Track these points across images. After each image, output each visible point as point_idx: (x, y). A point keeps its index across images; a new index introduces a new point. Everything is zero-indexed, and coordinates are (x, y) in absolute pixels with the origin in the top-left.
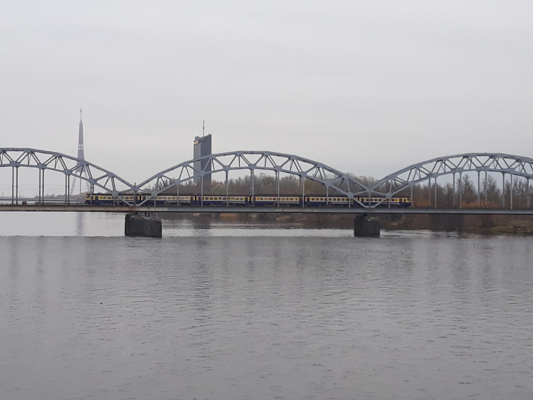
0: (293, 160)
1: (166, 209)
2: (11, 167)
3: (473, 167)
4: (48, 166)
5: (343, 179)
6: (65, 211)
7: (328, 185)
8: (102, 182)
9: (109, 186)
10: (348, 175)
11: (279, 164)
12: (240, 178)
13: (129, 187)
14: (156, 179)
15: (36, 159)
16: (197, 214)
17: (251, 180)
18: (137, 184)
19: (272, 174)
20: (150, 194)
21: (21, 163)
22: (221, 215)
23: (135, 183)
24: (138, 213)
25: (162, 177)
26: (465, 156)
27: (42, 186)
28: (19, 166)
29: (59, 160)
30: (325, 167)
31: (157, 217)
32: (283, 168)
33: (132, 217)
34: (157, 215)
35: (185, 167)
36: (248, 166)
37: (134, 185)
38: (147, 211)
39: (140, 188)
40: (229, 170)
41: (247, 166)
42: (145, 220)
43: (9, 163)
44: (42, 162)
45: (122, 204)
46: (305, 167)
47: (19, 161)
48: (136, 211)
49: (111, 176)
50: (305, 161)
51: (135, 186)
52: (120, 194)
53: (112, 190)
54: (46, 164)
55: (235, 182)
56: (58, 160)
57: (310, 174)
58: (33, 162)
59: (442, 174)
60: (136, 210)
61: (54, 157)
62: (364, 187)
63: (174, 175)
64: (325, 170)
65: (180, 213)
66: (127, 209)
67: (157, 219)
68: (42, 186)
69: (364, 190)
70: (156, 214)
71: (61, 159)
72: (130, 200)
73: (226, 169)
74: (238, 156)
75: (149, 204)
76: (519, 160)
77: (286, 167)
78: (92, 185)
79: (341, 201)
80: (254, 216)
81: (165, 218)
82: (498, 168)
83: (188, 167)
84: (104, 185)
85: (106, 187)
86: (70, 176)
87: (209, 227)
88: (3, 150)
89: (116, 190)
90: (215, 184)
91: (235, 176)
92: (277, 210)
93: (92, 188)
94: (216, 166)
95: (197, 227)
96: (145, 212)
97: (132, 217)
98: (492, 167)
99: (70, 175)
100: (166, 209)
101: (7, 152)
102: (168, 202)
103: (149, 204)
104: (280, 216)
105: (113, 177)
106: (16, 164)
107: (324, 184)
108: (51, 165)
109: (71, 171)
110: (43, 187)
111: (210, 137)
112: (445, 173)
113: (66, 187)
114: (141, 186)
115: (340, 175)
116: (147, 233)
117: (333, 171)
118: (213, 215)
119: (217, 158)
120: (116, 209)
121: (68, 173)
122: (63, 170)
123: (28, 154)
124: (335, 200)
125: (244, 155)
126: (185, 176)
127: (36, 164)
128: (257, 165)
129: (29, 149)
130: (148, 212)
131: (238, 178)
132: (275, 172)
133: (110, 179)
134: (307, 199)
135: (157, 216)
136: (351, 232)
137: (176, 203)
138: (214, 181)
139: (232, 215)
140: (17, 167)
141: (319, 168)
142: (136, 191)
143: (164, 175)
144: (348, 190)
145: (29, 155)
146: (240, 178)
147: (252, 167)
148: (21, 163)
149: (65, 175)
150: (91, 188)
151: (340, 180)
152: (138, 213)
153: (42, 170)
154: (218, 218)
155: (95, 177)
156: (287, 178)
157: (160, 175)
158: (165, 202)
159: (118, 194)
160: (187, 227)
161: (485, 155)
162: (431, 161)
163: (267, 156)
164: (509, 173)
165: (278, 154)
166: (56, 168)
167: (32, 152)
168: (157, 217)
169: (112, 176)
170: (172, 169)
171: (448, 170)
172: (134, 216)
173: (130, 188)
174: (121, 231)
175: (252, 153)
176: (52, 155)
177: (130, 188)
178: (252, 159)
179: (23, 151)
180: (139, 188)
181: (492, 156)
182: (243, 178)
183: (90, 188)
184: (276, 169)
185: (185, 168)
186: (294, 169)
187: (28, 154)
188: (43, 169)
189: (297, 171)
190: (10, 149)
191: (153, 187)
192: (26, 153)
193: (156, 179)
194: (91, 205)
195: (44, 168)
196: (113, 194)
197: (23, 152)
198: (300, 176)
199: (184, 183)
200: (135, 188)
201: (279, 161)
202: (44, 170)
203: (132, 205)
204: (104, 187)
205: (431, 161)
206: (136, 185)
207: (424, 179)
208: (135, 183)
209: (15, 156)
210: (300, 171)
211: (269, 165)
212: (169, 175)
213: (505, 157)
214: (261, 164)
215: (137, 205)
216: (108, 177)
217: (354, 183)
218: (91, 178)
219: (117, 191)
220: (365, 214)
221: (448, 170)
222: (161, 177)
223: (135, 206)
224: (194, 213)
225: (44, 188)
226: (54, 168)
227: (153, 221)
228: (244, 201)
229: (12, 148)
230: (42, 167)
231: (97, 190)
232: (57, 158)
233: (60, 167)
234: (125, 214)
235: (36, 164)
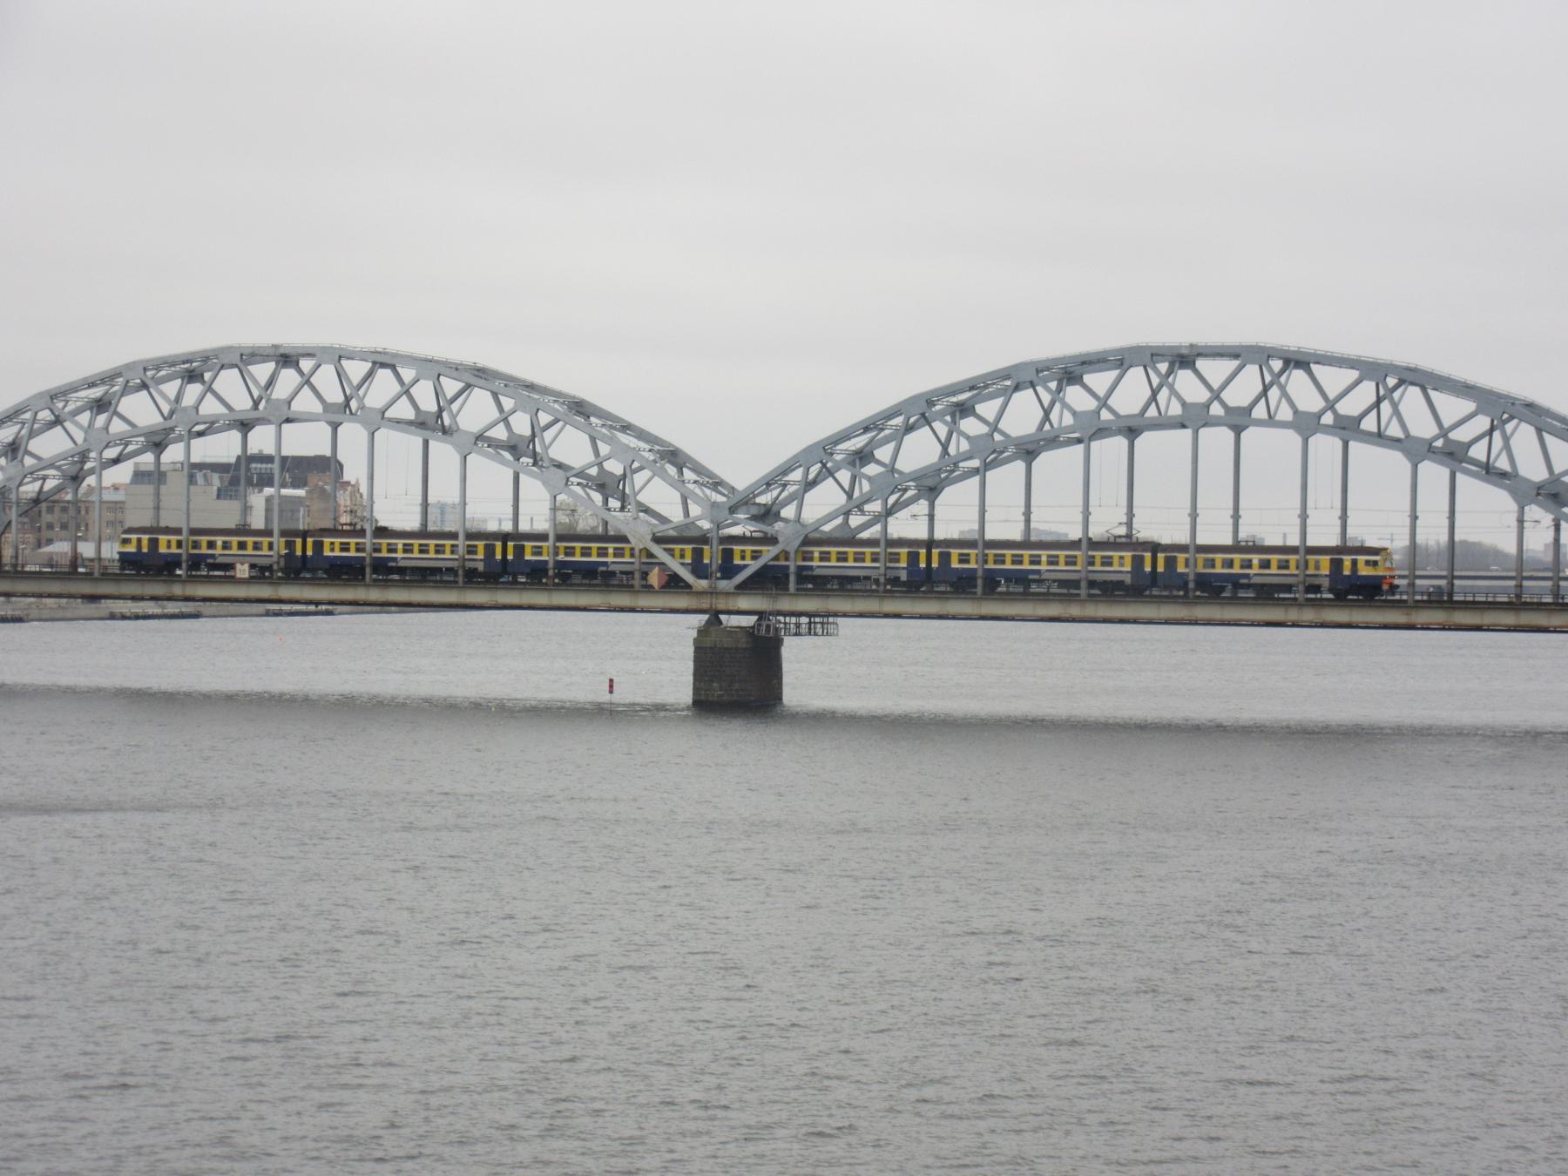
72: (434, 556)
79: (1274, 570)
102: (612, 568)
124: (1053, 561)
134: (515, 547)
137: (1288, 588)
194: (550, 582)
196: (634, 536)
228: (1127, 572)
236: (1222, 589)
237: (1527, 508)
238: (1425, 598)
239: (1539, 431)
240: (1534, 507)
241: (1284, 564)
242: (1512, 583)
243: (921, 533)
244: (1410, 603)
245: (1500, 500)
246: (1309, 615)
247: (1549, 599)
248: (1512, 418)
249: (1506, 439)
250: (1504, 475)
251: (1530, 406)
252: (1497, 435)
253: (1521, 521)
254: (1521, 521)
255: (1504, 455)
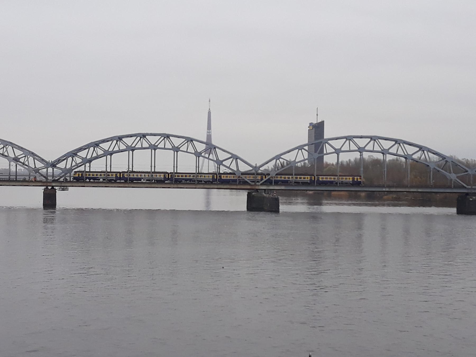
0: (399, 144)
1: (283, 188)
2: (150, 150)
4: (181, 149)
5: (447, 161)
6: (195, 188)
7: (432, 166)
8: (227, 163)
9: (234, 167)
10: (451, 158)
11: (386, 148)
12: (350, 160)
13: (251, 168)
14: (275, 160)
15: (171, 143)
16: (311, 192)
17: (360, 163)
18: (258, 165)
19: (380, 156)
20: (269, 174)
21: (158, 146)
22: (333, 193)
23: (256, 164)
24: (258, 190)
25: (280, 158)
27: (175, 166)
28: (157, 149)
29: (190, 144)
30: (429, 151)
31: (275, 195)
32: (390, 151)
33: (253, 194)
34: (275, 192)
35: (300, 150)
36: (357, 149)
37: (255, 166)
38: (266, 189)
39: (261, 169)
40: (340, 153)
41: (357, 149)
42: (264, 197)
43: (148, 146)
44: (176, 146)
45: (245, 183)
46: (411, 150)
47: (156, 144)
48: (257, 189)
49: (235, 158)
50: (411, 144)
51: (256, 167)
52: (243, 174)
53: (236, 170)
54: (179, 147)
55: (345, 163)
56: (189, 144)
57: (415, 157)
58: (168, 146)
60: (257, 188)
61: (186, 141)
62: (467, 169)
63: (290, 157)
64: (429, 153)
65: (295, 192)
66: (249, 187)
67: (275, 196)
68: (175, 166)
69: (467, 171)
70: (274, 192)
71: (192, 142)
73: (338, 152)
74: (348, 140)
75: (269, 182)
77: (393, 150)
78: (219, 166)
80: (363, 194)
81: (283, 195)
83: (303, 150)
84: (228, 166)
85: (230, 167)
86: (200, 158)
87: (320, 204)
88: (143, 135)
89: (240, 170)
90: (328, 165)
91: (345, 158)
92: (384, 190)
93: (219, 169)
94: (328, 149)
95: (310, 204)
96: (265, 190)
97: (253, 194)
99: (200, 157)
100: (283, 188)
101: (147, 137)
103: (269, 182)
104: (386, 195)
105: (237, 159)
106: (154, 147)
107: (428, 166)
108: (184, 148)
109: (200, 153)
110: (177, 167)
111: (322, 124)
113: (196, 167)
114: (261, 167)
115: (443, 157)
116: (266, 208)
117: (437, 154)
118: (325, 193)
119: (329, 142)
120: (239, 187)
121: (198, 155)
122: (194, 152)
123: (164, 139)
125: (354, 139)
126: (300, 158)
127: (171, 147)
128: (366, 148)
129: (165, 134)
130: (267, 190)
131: (347, 160)
132: (382, 155)
133: (234, 160)
135: (275, 193)
136: (454, 210)
138: (326, 163)
139: (342, 193)
140: (155, 150)
141: (423, 151)
142: (257, 172)
143: (282, 157)
144: (450, 171)
145: (165, 139)
146: (350, 160)
147: (361, 150)
148: (158, 146)
149: (195, 157)
150: (218, 168)
151: (443, 162)
152: (258, 190)
153: (176, 153)
154: (330, 196)
155: (221, 159)
156: (393, 160)
157: (278, 157)
158: (334, 182)
159: (241, 174)
160: (302, 203)
163: (375, 140)
165: (385, 138)
166: (188, 151)
167: (167, 136)
168: (275, 195)
169: (236, 158)
170: (289, 152)
172: (255, 193)
173: (251, 169)
174: (243, 207)
175: (361, 137)
176: (184, 140)
177: (251, 169)
178: (362, 143)
179: (160, 135)
180: (259, 168)
182: (352, 160)
183: (217, 168)
184: (384, 152)
185: (300, 151)
186: (400, 152)
187: (164, 139)
188: (177, 152)
189: (403, 154)
190: (149, 134)
191: (271, 168)
192: (163, 138)
193: (275, 160)
195: (177, 150)
197: (160, 137)
198: (406, 158)
199: (299, 165)
200: (256, 168)
201: (386, 145)
202: (178, 153)
203: (253, 183)
204: (229, 168)
206: (257, 166)
208: (256, 164)
209: (153, 140)
210: (406, 154)
211: (377, 148)
212: (286, 157)
214: (370, 147)
215: (257, 183)
216: (232, 159)
217: (457, 165)
218: (218, 159)
219: (240, 171)
220: (467, 194)
222: (279, 159)
223: (255, 185)
224: (308, 191)
225: (178, 168)
226: (186, 151)
227: (272, 198)
229: (151, 133)
230: (176, 149)
231: (223, 170)
232: (189, 142)
233: (191, 149)
234: (247, 191)
235: (171, 147)
236: (278, 182)
237: (11, 162)
238: (23, 180)
239: (13, 148)
240: (12, 162)
241: (281, 178)
242: (8, 177)
243: (83, 170)
244: (29, 181)
245: (6, 161)
246: (176, 186)
247: (15, 180)
248: (7, 145)
249: (7, 149)
250: (6, 156)
251: (11, 143)
252: (5, 148)
253: (10, 165)
254: (10, 165)
255: (6, 152)
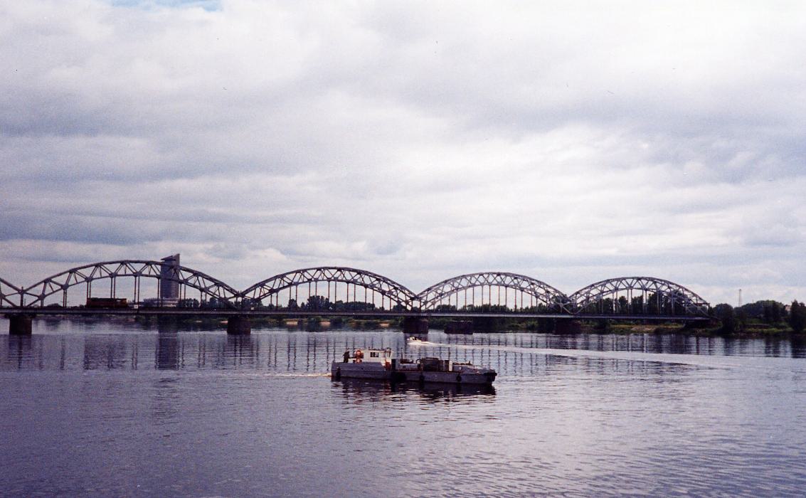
3: (325, 278)
26: (319, 269)
30: (204, 276)
59: (301, 283)
76: (359, 272)
82: (344, 279)
98: (340, 278)
112: (304, 282)
161: (335, 268)
162: (292, 272)
164: (352, 283)
171: (306, 280)
181: (339, 269)
200: (22, 292)
205: (292, 272)
207: (286, 287)
213: (350, 270)
218: (62, 286)
221: (306, 280)
